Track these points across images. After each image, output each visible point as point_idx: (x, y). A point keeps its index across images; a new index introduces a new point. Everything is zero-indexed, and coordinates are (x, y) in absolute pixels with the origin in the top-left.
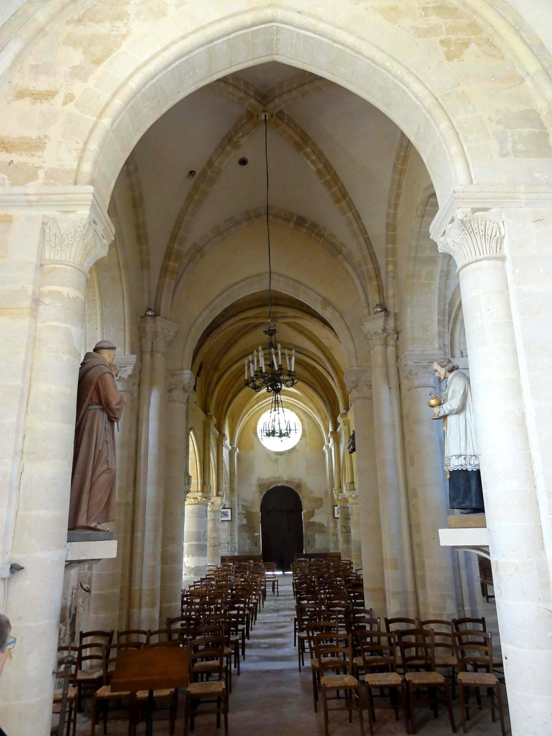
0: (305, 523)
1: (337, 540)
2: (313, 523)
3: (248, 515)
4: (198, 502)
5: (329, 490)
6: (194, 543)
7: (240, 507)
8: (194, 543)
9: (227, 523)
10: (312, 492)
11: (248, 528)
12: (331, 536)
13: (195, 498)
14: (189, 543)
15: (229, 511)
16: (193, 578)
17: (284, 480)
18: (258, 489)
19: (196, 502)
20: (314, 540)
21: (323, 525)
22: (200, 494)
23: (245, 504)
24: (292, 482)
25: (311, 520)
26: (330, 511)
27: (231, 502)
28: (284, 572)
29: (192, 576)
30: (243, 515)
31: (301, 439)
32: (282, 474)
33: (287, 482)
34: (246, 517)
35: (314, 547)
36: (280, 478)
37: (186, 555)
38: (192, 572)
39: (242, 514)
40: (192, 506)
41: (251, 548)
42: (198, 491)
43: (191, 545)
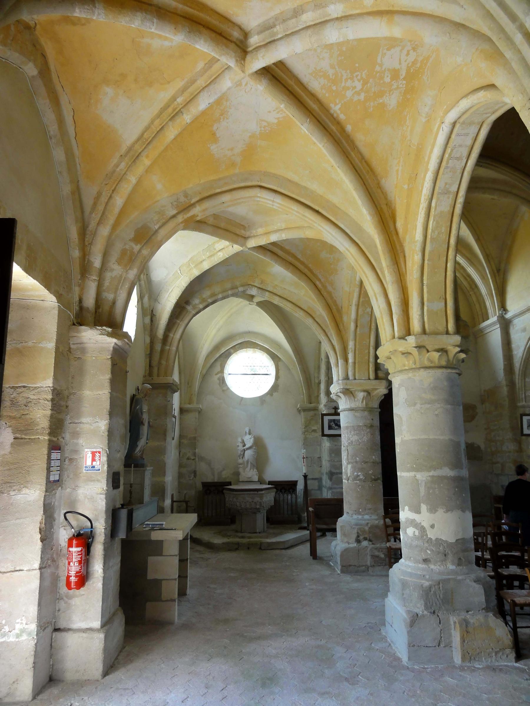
4: (448, 360)
6: (448, 472)
8: (448, 472)
13: (443, 351)
14: (432, 473)
16: (453, 572)
19: (444, 363)
21: (479, 447)
22: (457, 339)
29: (451, 567)
37: (407, 508)
38: (450, 557)
40: (432, 372)
42: (447, 333)
43: (441, 478)
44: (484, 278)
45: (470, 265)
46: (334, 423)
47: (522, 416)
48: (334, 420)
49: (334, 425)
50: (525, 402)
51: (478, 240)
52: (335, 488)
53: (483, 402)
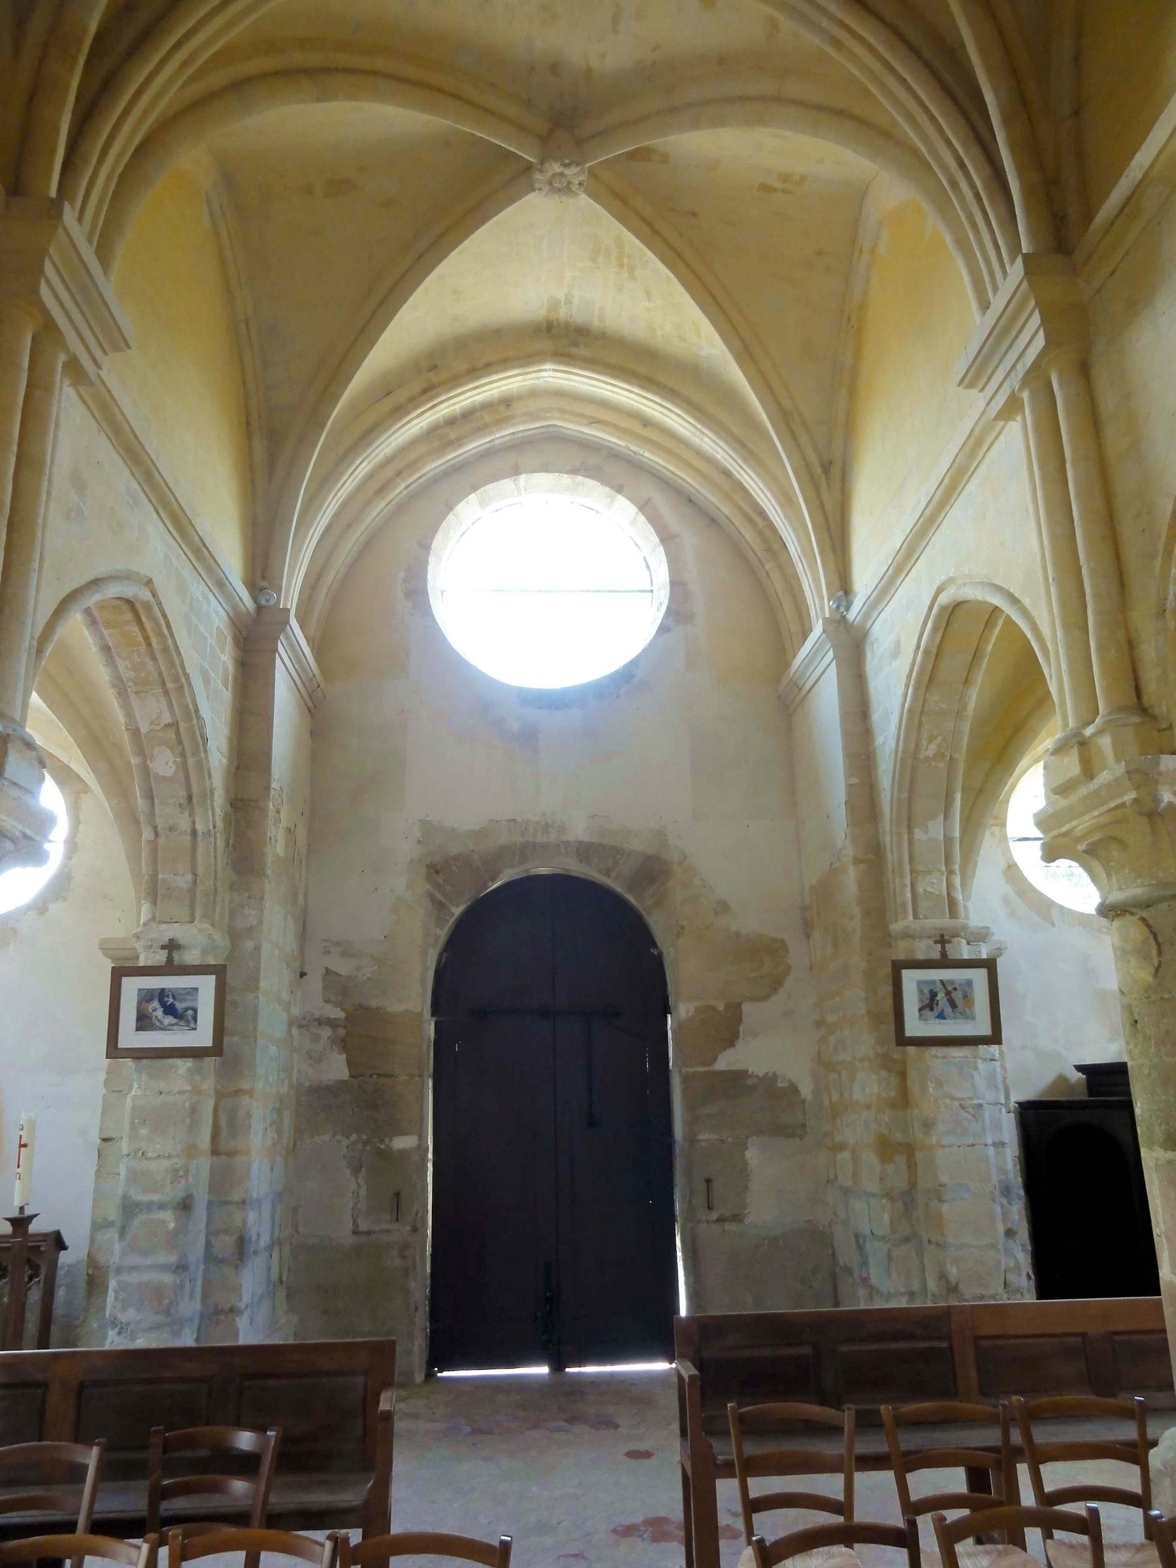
0: (686, 1080)
1: (913, 1185)
2: (736, 1080)
3: (358, 1029)
5: (851, 880)
7: (315, 983)
9: (183, 1065)
10: (723, 907)
11: (351, 1105)
12: (870, 1158)
15: (206, 985)
17: (571, 837)
18: (423, 887)
20: (743, 1172)
23: (343, 968)
24: (616, 851)
25: (725, 1061)
26: (855, 999)
27: (235, 935)
28: (558, 1367)
30: (326, 1033)
31: (663, 629)
32: (565, 813)
33: (585, 851)
34: (343, 1044)
35: (737, 1218)
36: (546, 828)
39: (322, 1022)
41: (364, 1226)
44: (786, 500)
45: (745, 460)
46: (163, 1004)
47: (898, 967)
48: (162, 994)
49: (159, 1013)
50: (916, 917)
51: (745, 354)
52: (136, 1268)
53: (807, 928)
